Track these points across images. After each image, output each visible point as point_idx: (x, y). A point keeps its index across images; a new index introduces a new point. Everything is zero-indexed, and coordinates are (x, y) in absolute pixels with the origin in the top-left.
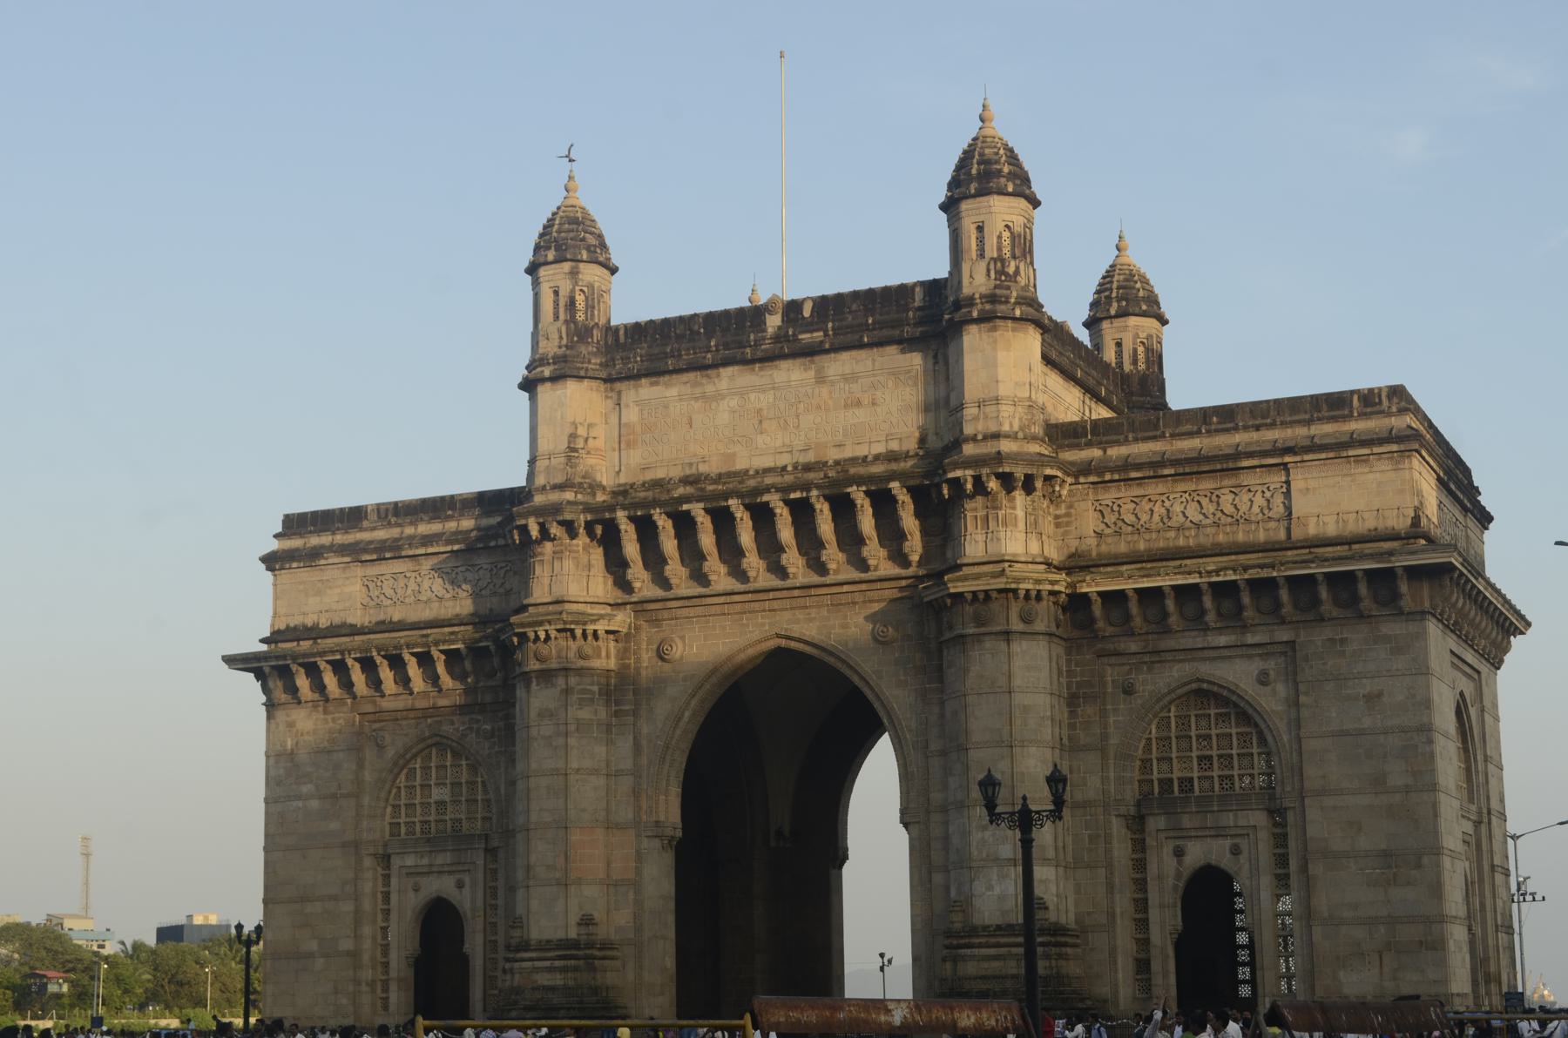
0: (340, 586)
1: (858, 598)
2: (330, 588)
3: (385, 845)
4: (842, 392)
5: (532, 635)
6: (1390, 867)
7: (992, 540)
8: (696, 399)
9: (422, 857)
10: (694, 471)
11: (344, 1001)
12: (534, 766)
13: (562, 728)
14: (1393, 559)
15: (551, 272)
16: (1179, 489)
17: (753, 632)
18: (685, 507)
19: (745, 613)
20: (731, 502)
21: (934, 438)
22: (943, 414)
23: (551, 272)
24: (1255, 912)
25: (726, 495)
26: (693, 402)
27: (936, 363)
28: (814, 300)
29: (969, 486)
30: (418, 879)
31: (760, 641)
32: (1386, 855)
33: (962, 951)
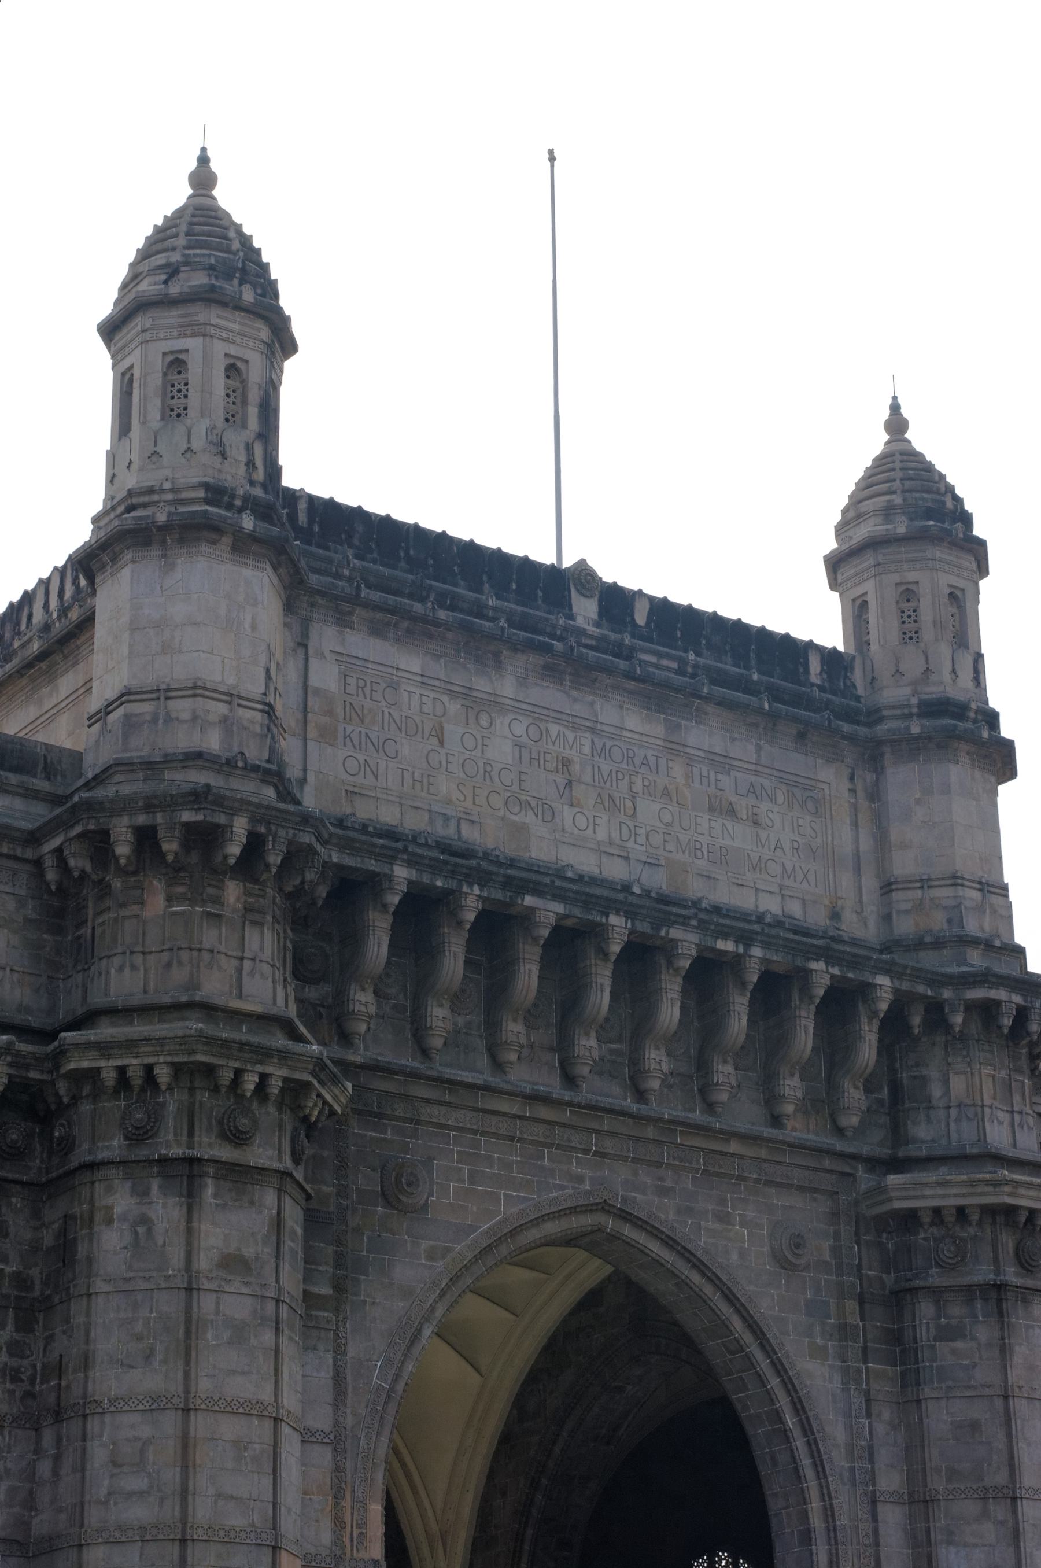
4: (705, 780)
5: (226, 1076)
7: (1021, 1125)
8: (453, 695)
10: (451, 831)
12: (204, 1385)
13: (270, 1306)
15: (235, 327)
17: (562, 1188)
18: (529, 900)
19: (550, 1146)
20: (614, 920)
21: (854, 917)
22: (870, 883)
23: (235, 327)
26: (445, 698)
27: (852, 791)
28: (651, 599)
29: (1007, 1022)
31: (574, 1210)
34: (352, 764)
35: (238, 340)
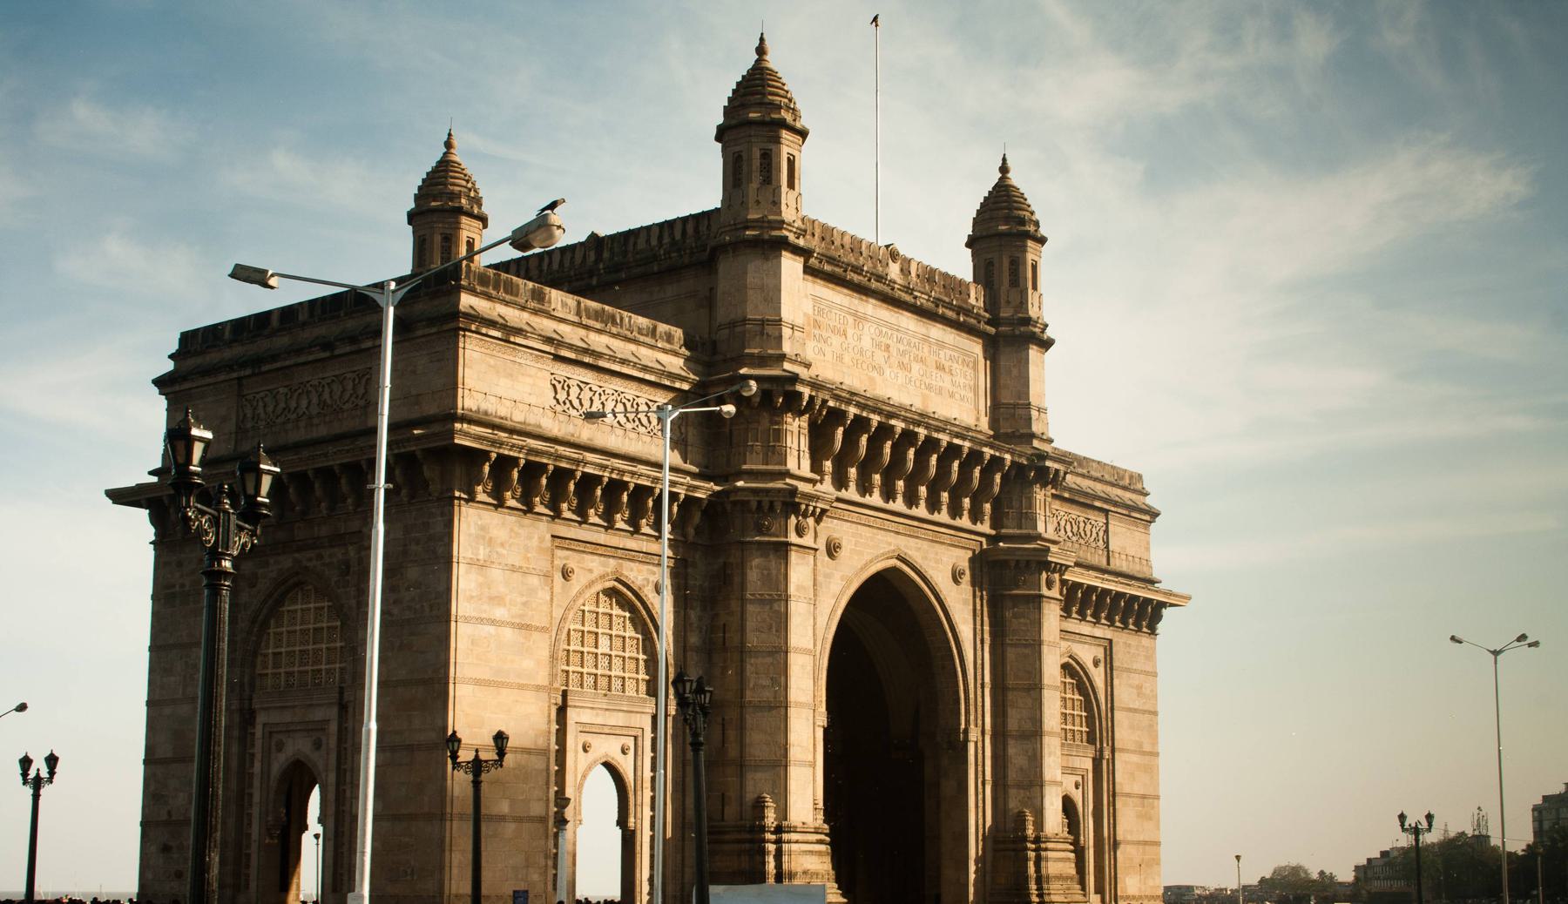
0: (530, 376)
1: (947, 539)
2: (523, 375)
3: (565, 694)
6: (1143, 807)
8: (850, 314)
9: (597, 715)
11: (535, 877)
14: (1172, 597)
16: (1064, 509)
18: (893, 422)
24: (1086, 832)
25: (919, 426)
26: (847, 316)
30: (589, 738)
32: (1144, 797)
33: (1043, 853)
34: (816, 349)
35: (792, 145)
